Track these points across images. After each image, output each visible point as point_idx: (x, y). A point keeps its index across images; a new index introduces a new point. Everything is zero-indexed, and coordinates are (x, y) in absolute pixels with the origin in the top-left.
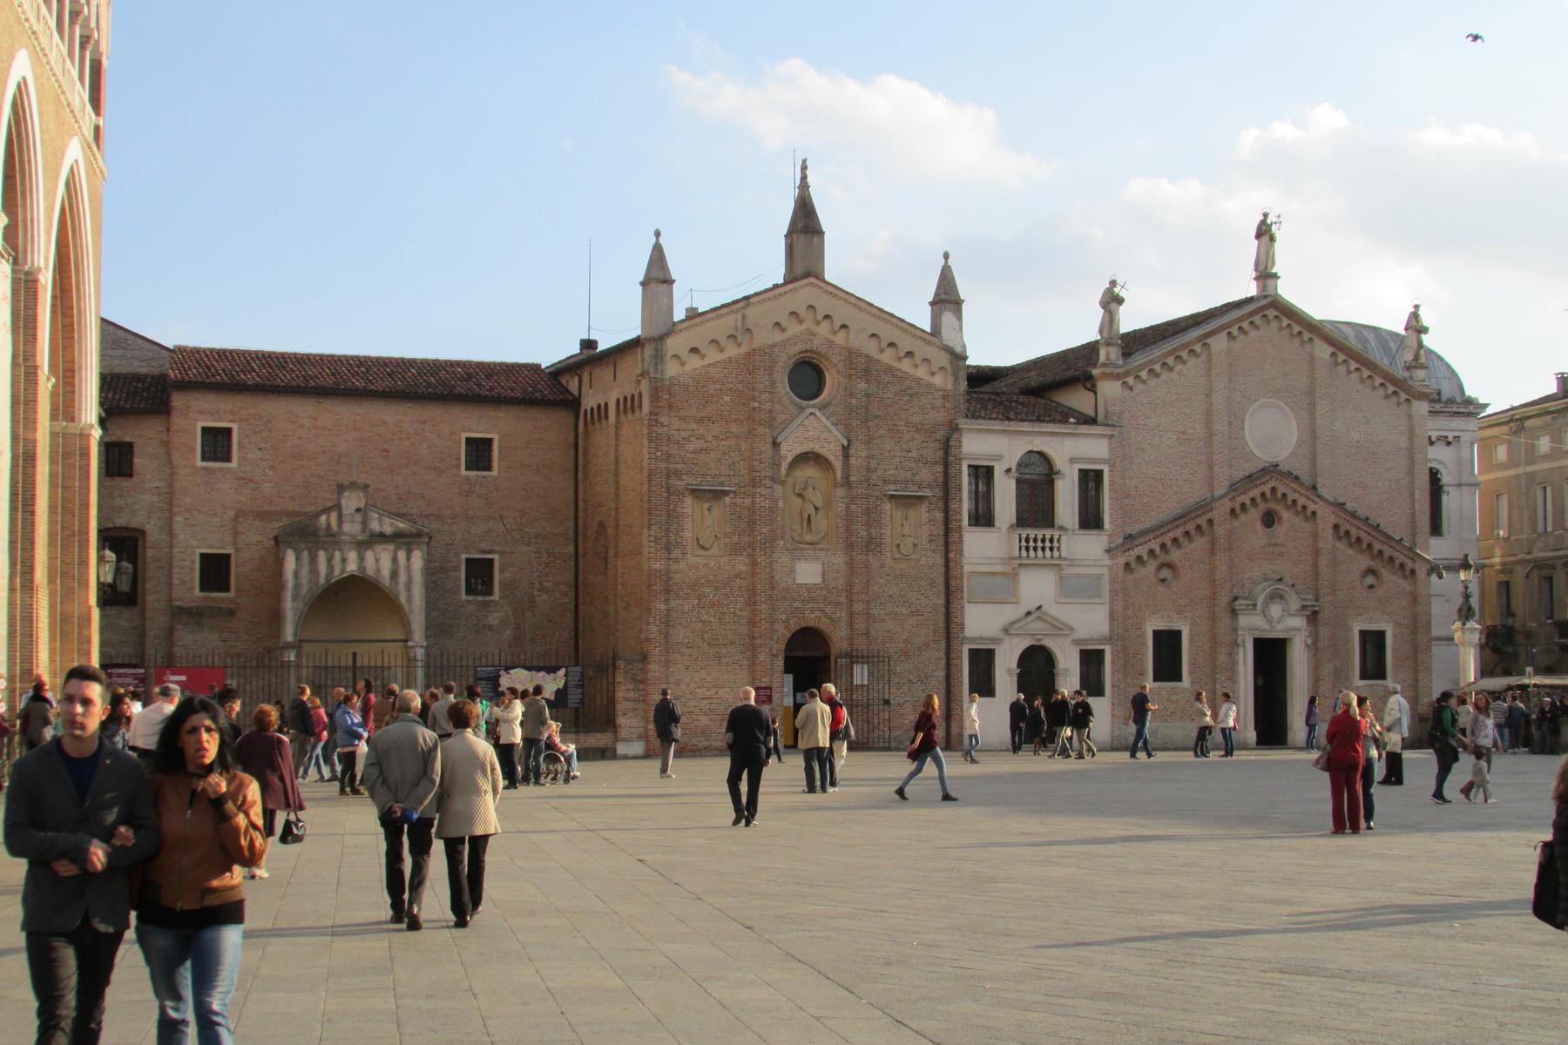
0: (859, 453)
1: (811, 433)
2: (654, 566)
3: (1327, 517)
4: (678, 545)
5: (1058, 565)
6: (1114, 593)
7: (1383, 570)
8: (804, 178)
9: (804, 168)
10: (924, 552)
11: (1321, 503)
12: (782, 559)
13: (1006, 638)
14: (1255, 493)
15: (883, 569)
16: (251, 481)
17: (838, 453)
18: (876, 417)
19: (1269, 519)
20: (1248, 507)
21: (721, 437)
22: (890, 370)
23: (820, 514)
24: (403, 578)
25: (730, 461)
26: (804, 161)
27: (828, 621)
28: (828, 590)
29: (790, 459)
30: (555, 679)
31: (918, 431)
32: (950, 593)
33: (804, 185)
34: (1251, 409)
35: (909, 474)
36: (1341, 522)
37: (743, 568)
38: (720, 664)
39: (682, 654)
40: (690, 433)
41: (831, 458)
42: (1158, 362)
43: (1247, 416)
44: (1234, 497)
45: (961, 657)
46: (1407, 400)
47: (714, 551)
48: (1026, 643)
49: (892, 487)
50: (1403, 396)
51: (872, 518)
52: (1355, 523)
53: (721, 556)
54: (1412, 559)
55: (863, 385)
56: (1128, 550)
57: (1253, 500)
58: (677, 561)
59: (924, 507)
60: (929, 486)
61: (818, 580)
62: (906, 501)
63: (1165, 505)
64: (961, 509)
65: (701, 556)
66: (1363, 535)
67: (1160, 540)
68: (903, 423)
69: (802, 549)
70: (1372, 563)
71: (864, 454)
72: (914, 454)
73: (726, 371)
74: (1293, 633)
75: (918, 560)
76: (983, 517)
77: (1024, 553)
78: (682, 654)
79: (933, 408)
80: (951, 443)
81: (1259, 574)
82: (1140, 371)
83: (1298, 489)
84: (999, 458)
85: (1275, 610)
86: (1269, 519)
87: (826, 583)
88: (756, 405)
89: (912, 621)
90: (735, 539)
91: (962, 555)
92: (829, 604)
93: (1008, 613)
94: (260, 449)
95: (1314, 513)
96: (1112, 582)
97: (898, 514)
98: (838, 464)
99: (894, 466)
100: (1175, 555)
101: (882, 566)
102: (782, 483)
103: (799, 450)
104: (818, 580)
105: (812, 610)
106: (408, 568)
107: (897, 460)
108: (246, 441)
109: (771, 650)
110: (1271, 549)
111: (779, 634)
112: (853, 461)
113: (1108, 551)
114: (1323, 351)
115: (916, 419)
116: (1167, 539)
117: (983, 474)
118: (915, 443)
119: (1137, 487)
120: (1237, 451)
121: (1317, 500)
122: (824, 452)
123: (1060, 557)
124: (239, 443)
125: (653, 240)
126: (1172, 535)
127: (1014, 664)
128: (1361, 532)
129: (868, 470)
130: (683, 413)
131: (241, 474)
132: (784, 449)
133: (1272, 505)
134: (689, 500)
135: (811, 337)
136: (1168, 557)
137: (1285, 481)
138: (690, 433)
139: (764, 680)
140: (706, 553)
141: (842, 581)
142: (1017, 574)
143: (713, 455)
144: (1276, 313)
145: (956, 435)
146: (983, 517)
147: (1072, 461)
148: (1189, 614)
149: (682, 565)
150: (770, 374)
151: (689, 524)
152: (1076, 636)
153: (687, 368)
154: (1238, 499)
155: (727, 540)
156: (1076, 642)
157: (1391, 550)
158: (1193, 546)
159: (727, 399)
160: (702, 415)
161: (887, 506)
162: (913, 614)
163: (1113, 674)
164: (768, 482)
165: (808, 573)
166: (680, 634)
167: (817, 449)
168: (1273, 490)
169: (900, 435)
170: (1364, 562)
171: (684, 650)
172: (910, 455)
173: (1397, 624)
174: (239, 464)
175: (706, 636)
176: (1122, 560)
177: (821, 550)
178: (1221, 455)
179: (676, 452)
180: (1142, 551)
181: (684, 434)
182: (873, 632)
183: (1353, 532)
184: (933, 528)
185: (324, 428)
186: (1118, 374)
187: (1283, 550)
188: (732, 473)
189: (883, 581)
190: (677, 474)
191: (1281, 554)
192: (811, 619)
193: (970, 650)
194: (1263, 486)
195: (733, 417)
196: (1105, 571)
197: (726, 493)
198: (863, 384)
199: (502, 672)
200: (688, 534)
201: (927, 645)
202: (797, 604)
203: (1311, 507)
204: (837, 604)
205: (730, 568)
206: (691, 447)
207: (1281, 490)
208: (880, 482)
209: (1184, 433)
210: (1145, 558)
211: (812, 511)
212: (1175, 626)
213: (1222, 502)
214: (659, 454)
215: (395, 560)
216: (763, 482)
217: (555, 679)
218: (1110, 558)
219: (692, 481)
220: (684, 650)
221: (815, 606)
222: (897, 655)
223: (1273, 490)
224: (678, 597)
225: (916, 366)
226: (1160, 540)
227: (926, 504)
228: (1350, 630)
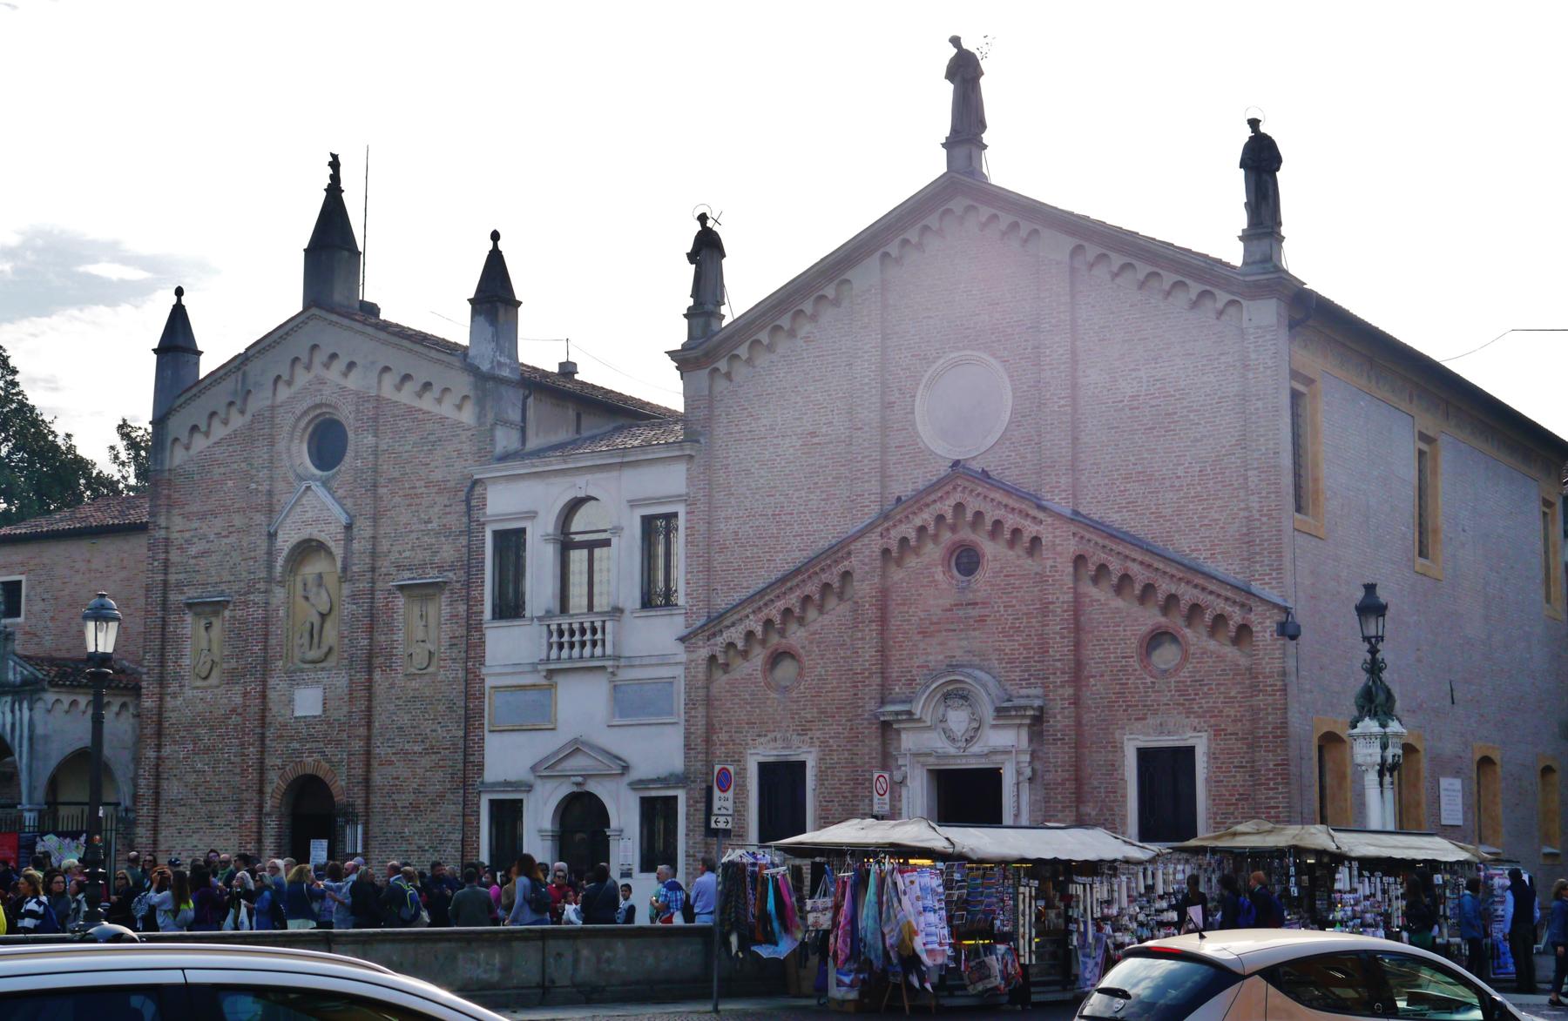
0: (364, 529)
1: (309, 515)
2: (146, 705)
3: (1061, 544)
4: (179, 677)
5: (603, 668)
6: (690, 704)
7: (1188, 632)
8: (335, 178)
9: (335, 164)
10: (442, 663)
11: (1049, 520)
12: (277, 684)
13: (539, 782)
14: (926, 517)
15: (393, 691)
16: (35, 635)
17: (339, 537)
18: (390, 480)
19: (966, 560)
20: (913, 543)
21: (224, 533)
22: (411, 410)
23: (328, 625)
24: (17, 733)
25: (231, 563)
26: (335, 157)
27: (327, 766)
28: (329, 724)
29: (285, 553)
30: (77, 847)
31: (440, 492)
32: (471, 720)
33: (334, 190)
34: (927, 376)
35: (427, 554)
36: (1088, 549)
37: (238, 700)
38: (212, 826)
39: (175, 814)
40: (192, 533)
41: (331, 544)
42: (762, 328)
43: (921, 387)
44: (888, 529)
45: (478, 813)
46: (1231, 303)
47: (213, 680)
48: (565, 789)
49: (407, 574)
50: (1223, 297)
51: (373, 621)
52: (1120, 548)
53: (218, 687)
54: (1243, 605)
55: (370, 439)
56: (714, 635)
57: (922, 530)
58: (174, 696)
59: (444, 599)
60: (452, 568)
61: (318, 711)
62: (422, 592)
63: (781, 555)
64: (482, 595)
65: (197, 688)
66: (1134, 569)
67: (763, 615)
68: (422, 483)
69: (302, 671)
70: (1162, 620)
71: (368, 533)
72: (434, 525)
73: (231, 449)
74: (999, 758)
75: (435, 674)
76: (510, 607)
77: (554, 653)
78: (175, 814)
79: (460, 453)
80: (474, 503)
81: (941, 657)
82: (736, 347)
83: (1005, 500)
84: (532, 515)
85: (958, 719)
86: (966, 560)
87: (328, 713)
88: (253, 486)
89: (426, 761)
90: (233, 663)
91: (483, 664)
92: (330, 742)
93: (540, 746)
94: (43, 600)
95: (1036, 541)
96: (689, 687)
97: (416, 610)
98: (338, 551)
99: (409, 546)
100: (797, 636)
101: (392, 686)
102: (281, 583)
103: (295, 538)
104: (318, 711)
105: (311, 752)
106: (21, 719)
107: (414, 535)
108: (32, 593)
109: (260, 807)
110: (961, 613)
111: (275, 785)
112: (356, 545)
113: (682, 639)
114: (1057, 248)
115: (438, 475)
116: (774, 612)
117: (511, 543)
118: (436, 510)
119: (736, 533)
120: (904, 451)
121: (1041, 515)
122: (322, 537)
123: (604, 656)
124: (27, 596)
125: (174, 300)
126: (781, 604)
127: (547, 823)
128: (1130, 564)
129: (374, 554)
130: (188, 509)
131: (27, 629)
132: (281, 536)
133: (966, 534)
134: (189, 618)
135: (321, 387)
136: (784, 641)
137: (980, 490)
138: (192, 533)
139: (249, 846)
140: (205, 683)
141: (345, 709)
142: (553, 686)
143: (214, 557)
144: (968, 202)
145: (478, 490)
146: (510, 607)
147: (634, 504)
148: (818, 734)
149: (179, 701)
150: (272, 444)
151: (188, 649)
152: (634, 775)
153: (194, 451)
154: (893, 533)
155: (225, 666)
156: (636, 785)
157: (1196, 592)
158: (826, 619)
159: (230, 483)
160: (205, 508)
161: (401, 601)
162: (427, 752)
163: (687, 835)
164: (262, 586)
165: (308, 702)
166: (172, 789)
167: (316, 535)
168: (959, 508)
169: (418, 501)
170: (1150, 618)
171: (177, 809)
172: (430, 526)
173: (1217, 732)
174: (26, 618)
175: (200, 789)
176: (704, 653)
177: (323, 669)
178: (866, 461)
179: (179, 559)
180: (736, 635)
181: (187, 535)
182: (377, 778)
183: (1115, 566)
184: (455, 627)
185: (96, 570)
186: (697, 359)
187: (986, 611)
188: (232, 578)
189: (392, 707)
190: (180, 586)
191: (982, 620)
192: (310, 763)
193: (492, 802)
194: (938, 505)
195: (236, 506)
196: (679, 672)
197: (225, 604)
198: (370, 438)
199: (38, 839)
200: (186, 661)
201: (442, 796)
202: (296, 745)
203: (1030, 529)
204: (339, 742)
205: (226, 701)
206: (193, 550)
207: (973, 505)
208: (393, 570)
209: (813, 434)
210: (740, 645)
211: (316, 620)
212: (795, 756)
213: (866, 540)
214: (156, 564)
215: (13, 711)
216: (257, 586)
217: (77, 847)
218: (688, 650)
219: (191, 593)
220: (177, 809)
221: (314, 745)
222: (406, 811)
223: (959, 508)
224: (175, 742)
225: (439, 401)
226: (763, 615)
227: (447, 593)
228: (1117, 748)
